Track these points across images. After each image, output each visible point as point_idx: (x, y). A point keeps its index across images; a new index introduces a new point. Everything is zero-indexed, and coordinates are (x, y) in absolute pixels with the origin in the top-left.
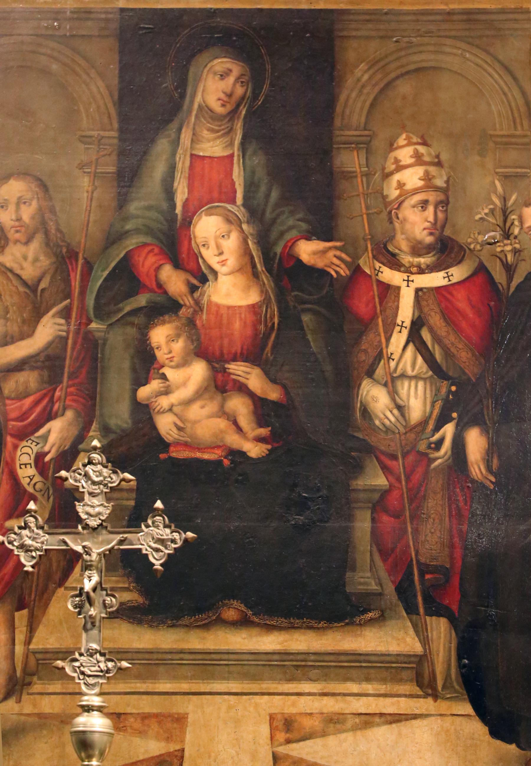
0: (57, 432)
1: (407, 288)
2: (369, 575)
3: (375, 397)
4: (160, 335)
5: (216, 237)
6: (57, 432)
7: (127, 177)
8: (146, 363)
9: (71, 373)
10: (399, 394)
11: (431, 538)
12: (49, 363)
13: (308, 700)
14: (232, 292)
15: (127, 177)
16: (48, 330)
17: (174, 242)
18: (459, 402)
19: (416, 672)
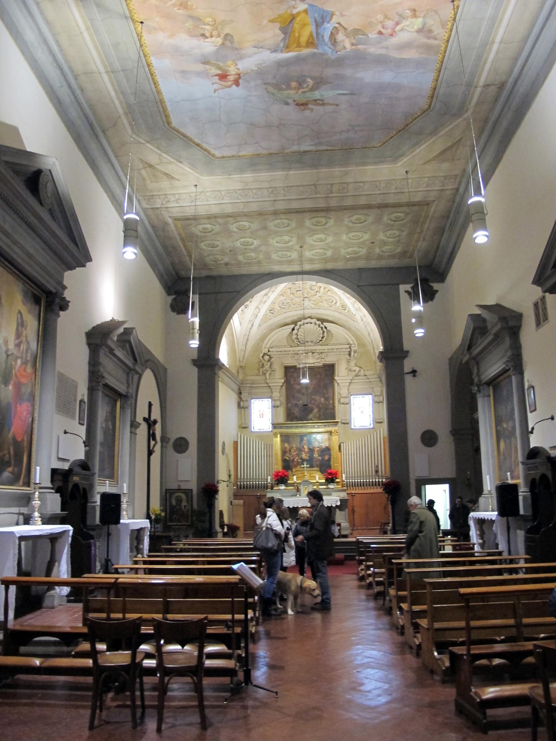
0: (297, 458)
1: (316, 449)
2: (314, 465)
3: (314, 455)
4: (303, 453)
5: (306, 447)
6: (297, 458)
7: (300, 444)
8: (302, 454)
9: (298, 455)
10: (316, 455)
11: (318, 463)
12: (296, 454)
13: (311, 472)
14: (306, 450)
15: (300, 444)
16: (296, 452)
17: (303, 447)
18: (319, 456)
19: (317, 470)
